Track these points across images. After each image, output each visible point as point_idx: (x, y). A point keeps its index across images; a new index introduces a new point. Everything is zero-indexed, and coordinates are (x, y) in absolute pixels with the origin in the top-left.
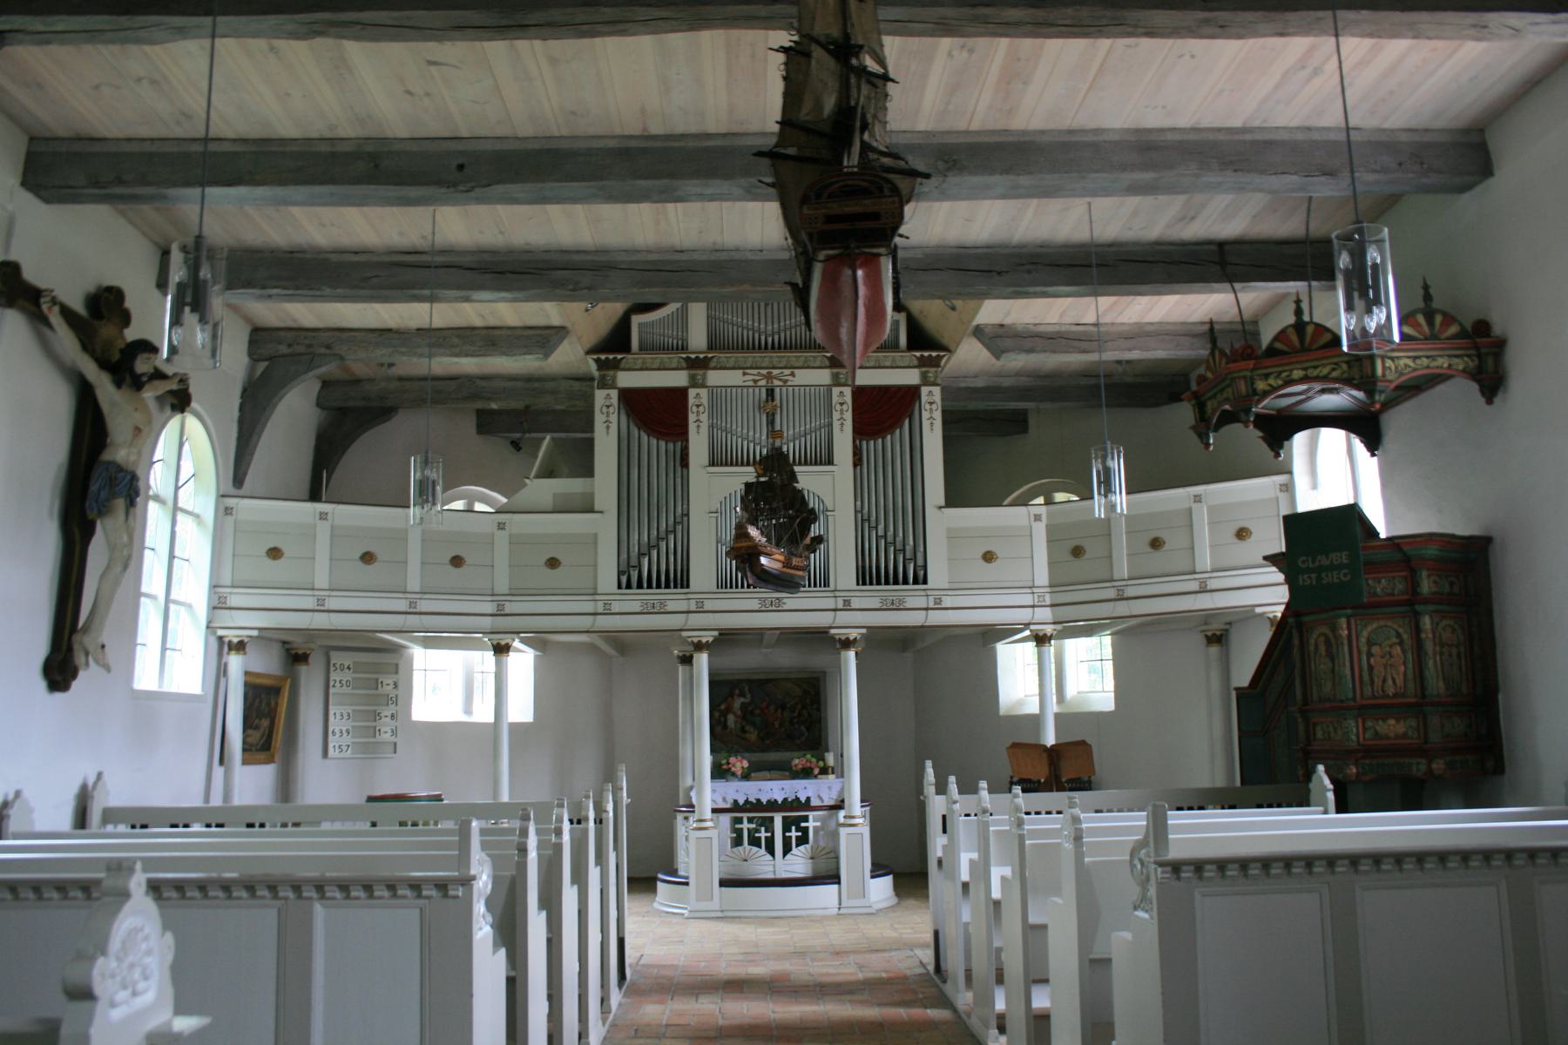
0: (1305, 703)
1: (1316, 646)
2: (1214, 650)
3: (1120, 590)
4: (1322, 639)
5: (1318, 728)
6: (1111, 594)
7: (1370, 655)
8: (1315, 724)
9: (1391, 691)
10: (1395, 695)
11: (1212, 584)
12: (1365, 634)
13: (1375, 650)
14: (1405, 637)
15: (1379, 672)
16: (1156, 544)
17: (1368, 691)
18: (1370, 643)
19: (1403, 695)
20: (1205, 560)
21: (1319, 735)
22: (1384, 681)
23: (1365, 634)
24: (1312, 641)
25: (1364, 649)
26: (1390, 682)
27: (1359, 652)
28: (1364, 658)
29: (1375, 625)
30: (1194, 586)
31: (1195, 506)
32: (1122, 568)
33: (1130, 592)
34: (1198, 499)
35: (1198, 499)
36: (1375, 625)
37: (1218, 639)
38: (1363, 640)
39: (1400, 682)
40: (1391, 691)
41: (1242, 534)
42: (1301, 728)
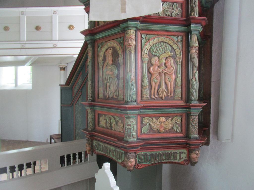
0: (93, 100)
1: (105, 58)
2: (62, 72)
3: (23, 45)
4: (110, 51)
5: (102, 118)
6: (19, 46)
7: (150, 63)
8: (99, 115)
9: (164, 94)
10: (167, 97)
11: (58, 45)
12: (148, 46)
13: (155, 60)
14: (178, 51)
15: (156, 80)
16: (38, 28)
17: (146, 93)
18: (151, 55)
19: (173, 98)
20: (56, 35)
21: (103, 123)
22: (160, 86)
23: (148, 46)
24: (102, 54)
25: (146, 59)
26: (164, 87)
27: (143, 62)
28: (145, 66)
29: (156, 40)
30: (52, 46)
31: (54, 15)
32: (24, 36)
33: (27, 46)
34: (55, 12)
35: (55, 12)
36: (156, 40)
37: (63, 69)
38: (146, 51)
39: (171, 86)
40: (164, 94)
41: (71, 27)
42: (90, 116)
